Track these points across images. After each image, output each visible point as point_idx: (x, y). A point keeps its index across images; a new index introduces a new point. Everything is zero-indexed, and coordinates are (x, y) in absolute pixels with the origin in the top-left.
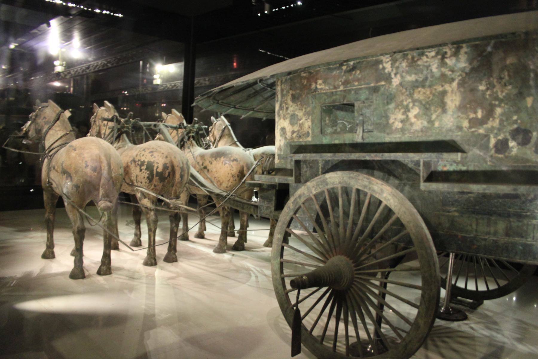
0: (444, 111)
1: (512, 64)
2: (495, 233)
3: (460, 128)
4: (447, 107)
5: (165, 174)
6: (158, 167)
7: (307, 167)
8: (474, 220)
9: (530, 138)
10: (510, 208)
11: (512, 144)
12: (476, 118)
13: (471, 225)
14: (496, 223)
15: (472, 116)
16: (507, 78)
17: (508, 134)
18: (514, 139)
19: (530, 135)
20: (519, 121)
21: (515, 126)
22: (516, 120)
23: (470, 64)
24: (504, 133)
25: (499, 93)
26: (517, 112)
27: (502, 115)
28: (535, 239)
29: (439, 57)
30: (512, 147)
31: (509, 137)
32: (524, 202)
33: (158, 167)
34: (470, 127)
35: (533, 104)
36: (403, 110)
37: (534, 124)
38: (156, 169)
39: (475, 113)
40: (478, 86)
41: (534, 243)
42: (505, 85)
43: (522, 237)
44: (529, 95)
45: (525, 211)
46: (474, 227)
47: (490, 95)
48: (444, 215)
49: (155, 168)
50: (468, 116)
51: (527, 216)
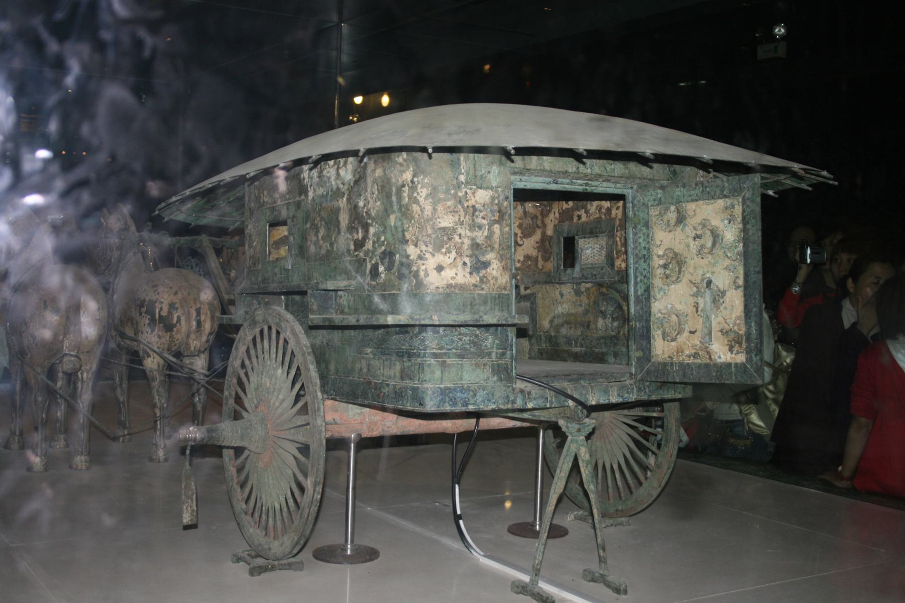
0: (339, 232)
1: (380, 177)
2: (395, 376)
3: (349, 251)
4: (341, 227)
5: (172, 319)
6: (161, 309)
7: (260, 303)
8: (382, 361)
9: (394, 261)
10: (403, 345)
11: (381, 269)
12: (357, 239)
13: (380, 369)
14: (395, 364)
15: (356, 237)
16: (376, 192)
17: (378, 258)
18: (382, 263)
19: (394, 258)
20: (386, 243)
21: (383, 248)
22: (383, 242)
23: (354, 176)
24: (376, 256)
25: (372, 210)
26: (384, 232)
27: (374, 235)
28: (421, 380)
29: (336, 167)
30: (381, 273)
31: (379, 262)
32: (412, 338)
33: (161, 309)
34: (355, 250)
35: (395, 223)
36: (315, 231)
37: (397, 246)
38: (159, 312)
39: (358, 233)
40: (358, 202)
41: (420, 386)
42: (376, 202)
43: (411, 379)
44: (393, 212)
45: (413, 348)
46: (382, 371)
47: (366, 212)
48: (363, 358)
49: (157, 311)
50: (353, 237)
51: (414, 353)
